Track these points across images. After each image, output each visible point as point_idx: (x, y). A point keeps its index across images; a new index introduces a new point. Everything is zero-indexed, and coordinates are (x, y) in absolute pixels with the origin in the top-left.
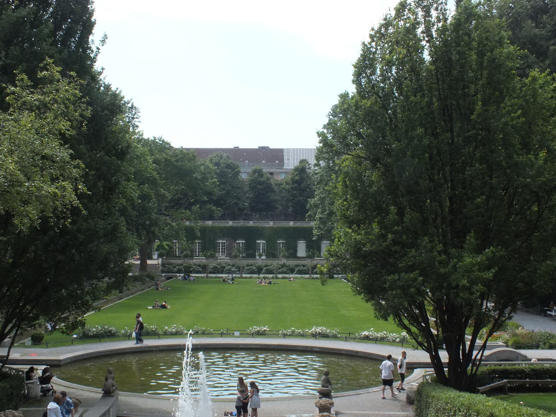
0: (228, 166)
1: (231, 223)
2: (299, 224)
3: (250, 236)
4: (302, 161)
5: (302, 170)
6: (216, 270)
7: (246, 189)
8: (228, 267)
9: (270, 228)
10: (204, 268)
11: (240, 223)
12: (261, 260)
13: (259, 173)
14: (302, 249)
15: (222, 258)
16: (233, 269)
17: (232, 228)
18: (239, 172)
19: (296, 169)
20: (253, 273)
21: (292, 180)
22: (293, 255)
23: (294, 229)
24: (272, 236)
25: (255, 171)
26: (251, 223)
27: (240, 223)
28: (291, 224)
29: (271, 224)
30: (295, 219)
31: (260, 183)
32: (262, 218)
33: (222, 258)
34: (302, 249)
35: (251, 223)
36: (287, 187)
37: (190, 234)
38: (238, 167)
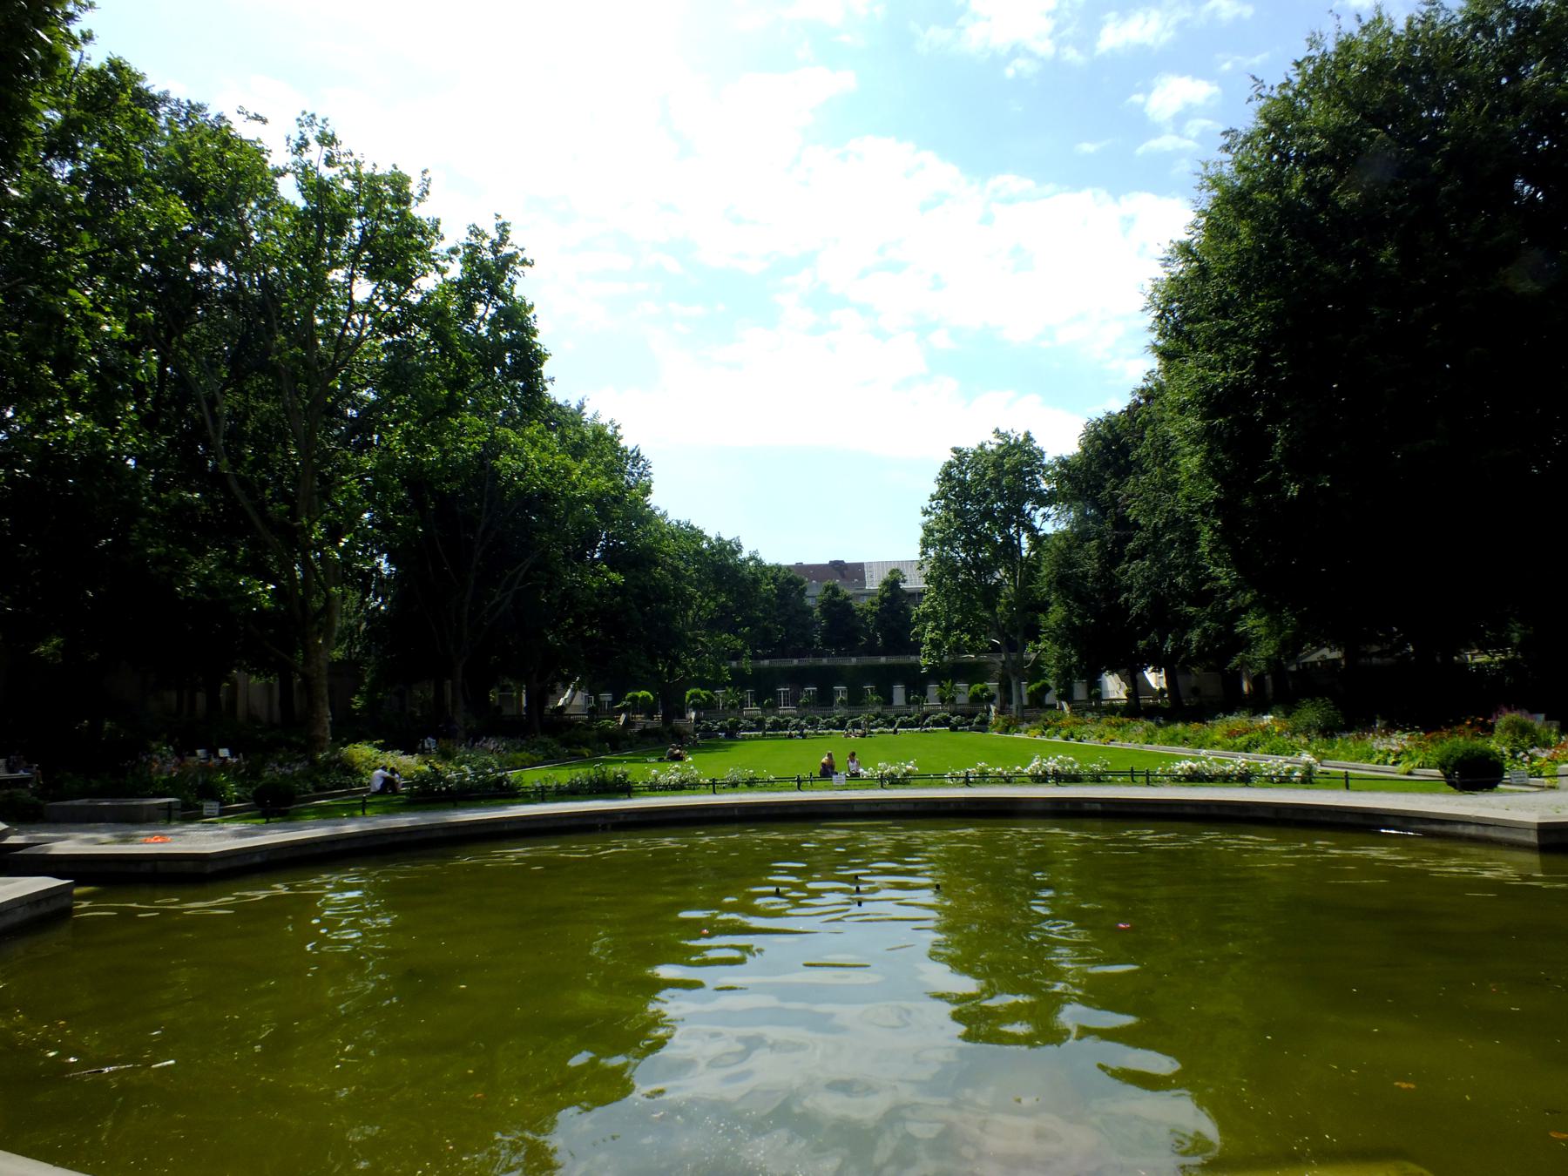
0: (790, 581)
1: (796, 662)
2: (894, 660)
3: (825, 680)
4: (893, 572)
5: (893, 583)
6: (776, 726)
7: (817, 612)
8: (794, 721)
9: (855, 667)
10: (760, 724)
11: (809, 661)
12: (840, 712)
13: (835, 591)
14: (899, 693)
15: (786, 710)
16: (803, 723)
17: (797, 668)
18: (802, 592)
19: (885, 583)
20: (829, 726)
21: (881, 597)
22: (888, 701)
23: (888, 668)
24: (855, 681)
25: (827, 589)
26: (825, 661)
27: (809, 661)
28: (883, 660)
29: (854, 660)
30: (885, 652)
31: (836, 604)
32: (838, 654)
33: (786, 710)
34: (899, 693)
35: (825, 661)
36: (875, 608)
37: (740, 680)
38: (802, 582)
